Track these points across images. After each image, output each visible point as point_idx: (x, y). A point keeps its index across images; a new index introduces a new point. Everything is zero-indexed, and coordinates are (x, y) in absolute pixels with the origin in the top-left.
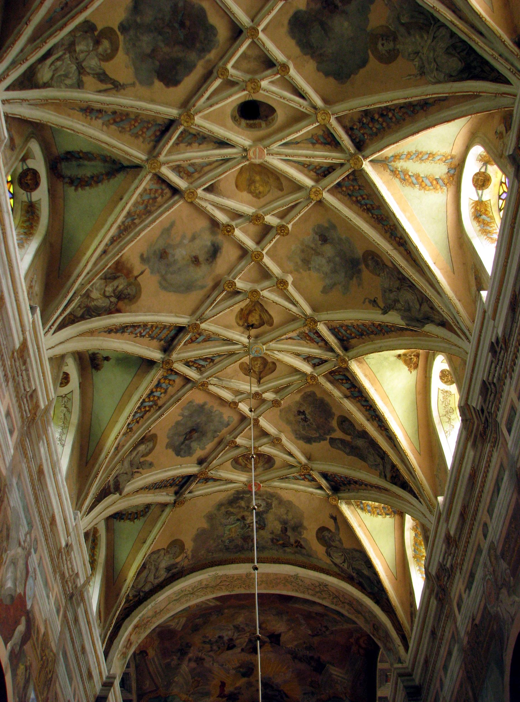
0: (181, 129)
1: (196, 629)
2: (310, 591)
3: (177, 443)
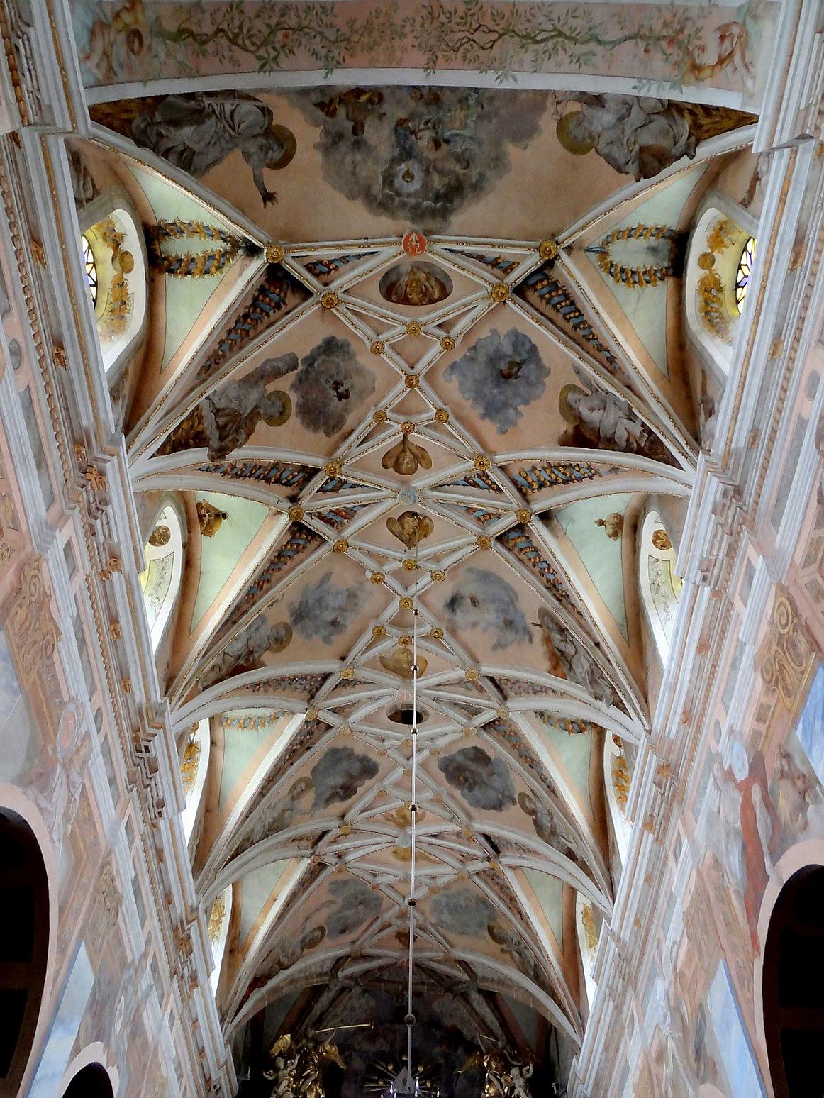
2: (292, 21)
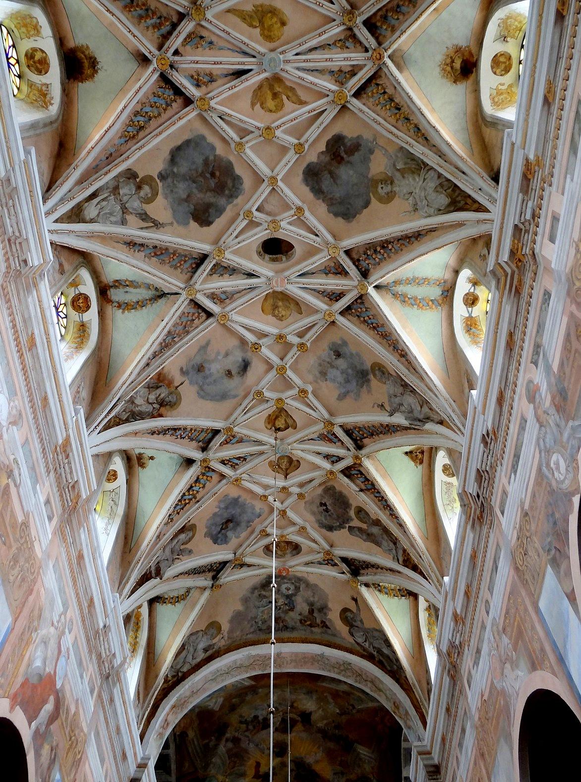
0: (214, 262)
1: (233, 708)
2: (336, 670)
3: (214, 533)
